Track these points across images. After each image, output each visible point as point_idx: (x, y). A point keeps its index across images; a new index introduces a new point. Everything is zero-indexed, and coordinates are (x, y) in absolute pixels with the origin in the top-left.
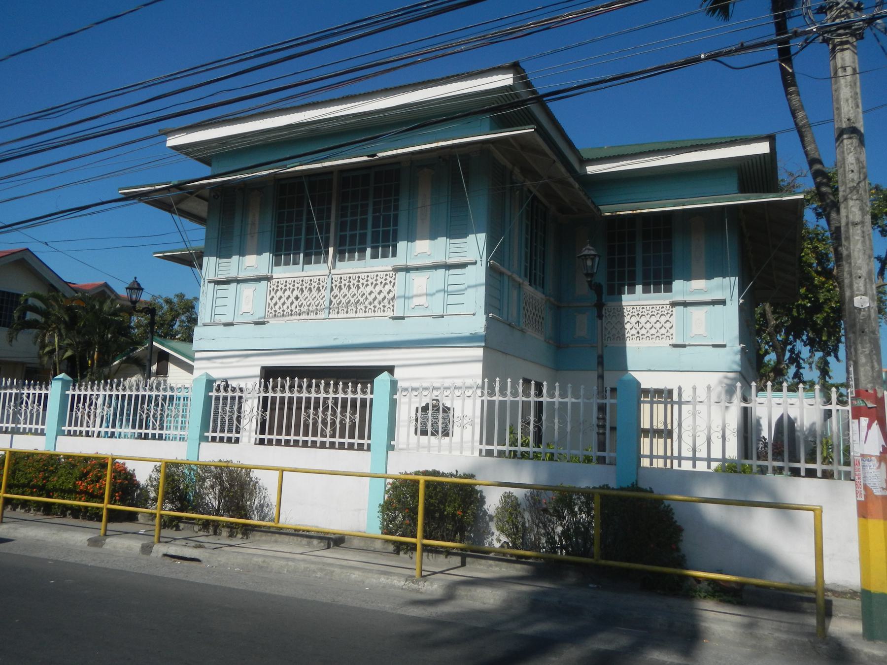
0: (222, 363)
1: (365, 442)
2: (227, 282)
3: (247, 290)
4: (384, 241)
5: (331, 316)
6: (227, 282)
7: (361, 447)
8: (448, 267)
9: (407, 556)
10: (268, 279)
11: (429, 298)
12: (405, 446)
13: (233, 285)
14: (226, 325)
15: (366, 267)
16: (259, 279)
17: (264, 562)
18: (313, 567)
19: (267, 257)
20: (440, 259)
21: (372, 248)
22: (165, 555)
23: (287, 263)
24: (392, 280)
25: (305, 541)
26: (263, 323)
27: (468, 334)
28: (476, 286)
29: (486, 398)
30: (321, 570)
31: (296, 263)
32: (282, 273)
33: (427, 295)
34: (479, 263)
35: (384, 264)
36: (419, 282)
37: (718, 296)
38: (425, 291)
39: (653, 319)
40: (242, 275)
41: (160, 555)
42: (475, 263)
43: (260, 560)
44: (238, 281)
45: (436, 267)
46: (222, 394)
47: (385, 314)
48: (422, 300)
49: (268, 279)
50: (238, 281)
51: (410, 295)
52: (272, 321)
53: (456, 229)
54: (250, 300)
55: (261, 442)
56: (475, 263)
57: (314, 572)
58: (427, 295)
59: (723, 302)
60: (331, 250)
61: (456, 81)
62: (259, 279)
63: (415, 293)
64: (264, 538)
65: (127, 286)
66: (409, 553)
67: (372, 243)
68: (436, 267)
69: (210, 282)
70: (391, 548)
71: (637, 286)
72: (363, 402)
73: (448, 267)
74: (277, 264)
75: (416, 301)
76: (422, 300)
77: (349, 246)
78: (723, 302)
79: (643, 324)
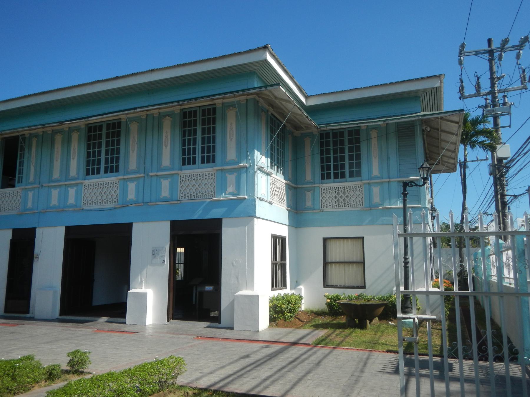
16: (268, 174)
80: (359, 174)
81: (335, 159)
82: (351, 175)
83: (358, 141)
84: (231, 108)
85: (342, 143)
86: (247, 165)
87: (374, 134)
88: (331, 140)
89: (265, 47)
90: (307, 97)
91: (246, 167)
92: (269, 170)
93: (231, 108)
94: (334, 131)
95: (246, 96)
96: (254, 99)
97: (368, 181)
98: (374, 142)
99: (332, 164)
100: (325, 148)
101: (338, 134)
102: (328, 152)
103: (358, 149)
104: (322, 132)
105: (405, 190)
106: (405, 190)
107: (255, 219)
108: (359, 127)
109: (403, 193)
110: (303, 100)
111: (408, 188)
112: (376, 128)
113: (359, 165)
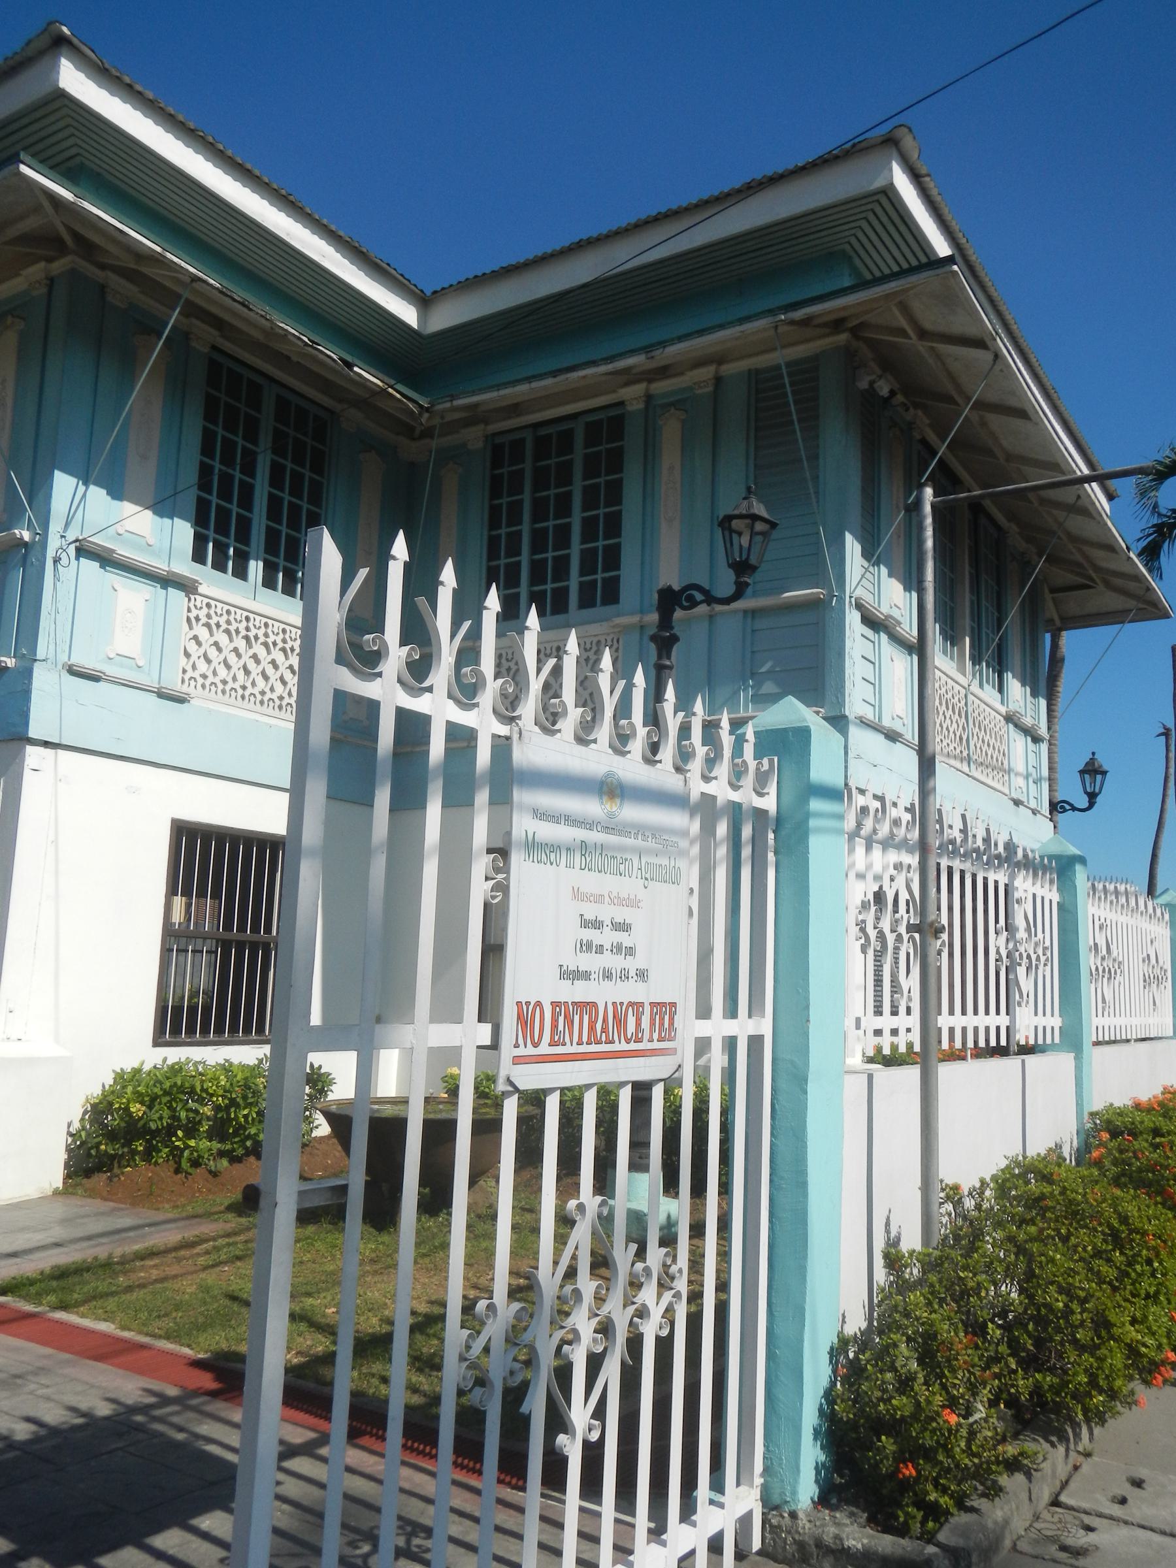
3: (134, 597)
10: (188, 587)
16: (167, 581)
19: (183, 532)
26: (180, 700)
80: (611, 595)
81: (539, 543)
82: (587, 601)
83: (616, 462)
84: (9, 320)
85: (565, 474)
86: (26, 535)
87: (671, 431)
88: (528, 466)
89: (59, 43)
90: (424, 301)
91: (26, 544)
92: (184, 567)
93: (9, 320)
94: (543, 432)
95: (42, 264)
96: (73, 272)
97: (635, 619)
98: (670, 458)
99: (525, 559)
100: (504, 501)
101: (552, 440)
102: (515, 517)
103: (615, 493)
104: (498, 440)
105: (665, 621)
106: (665, 621)
107: (30, 749)
108: (621, 404)
109: (653, 638)
110: (407, 313)
111: (679, 614)
112: (681, 403)
113: (613, 558)
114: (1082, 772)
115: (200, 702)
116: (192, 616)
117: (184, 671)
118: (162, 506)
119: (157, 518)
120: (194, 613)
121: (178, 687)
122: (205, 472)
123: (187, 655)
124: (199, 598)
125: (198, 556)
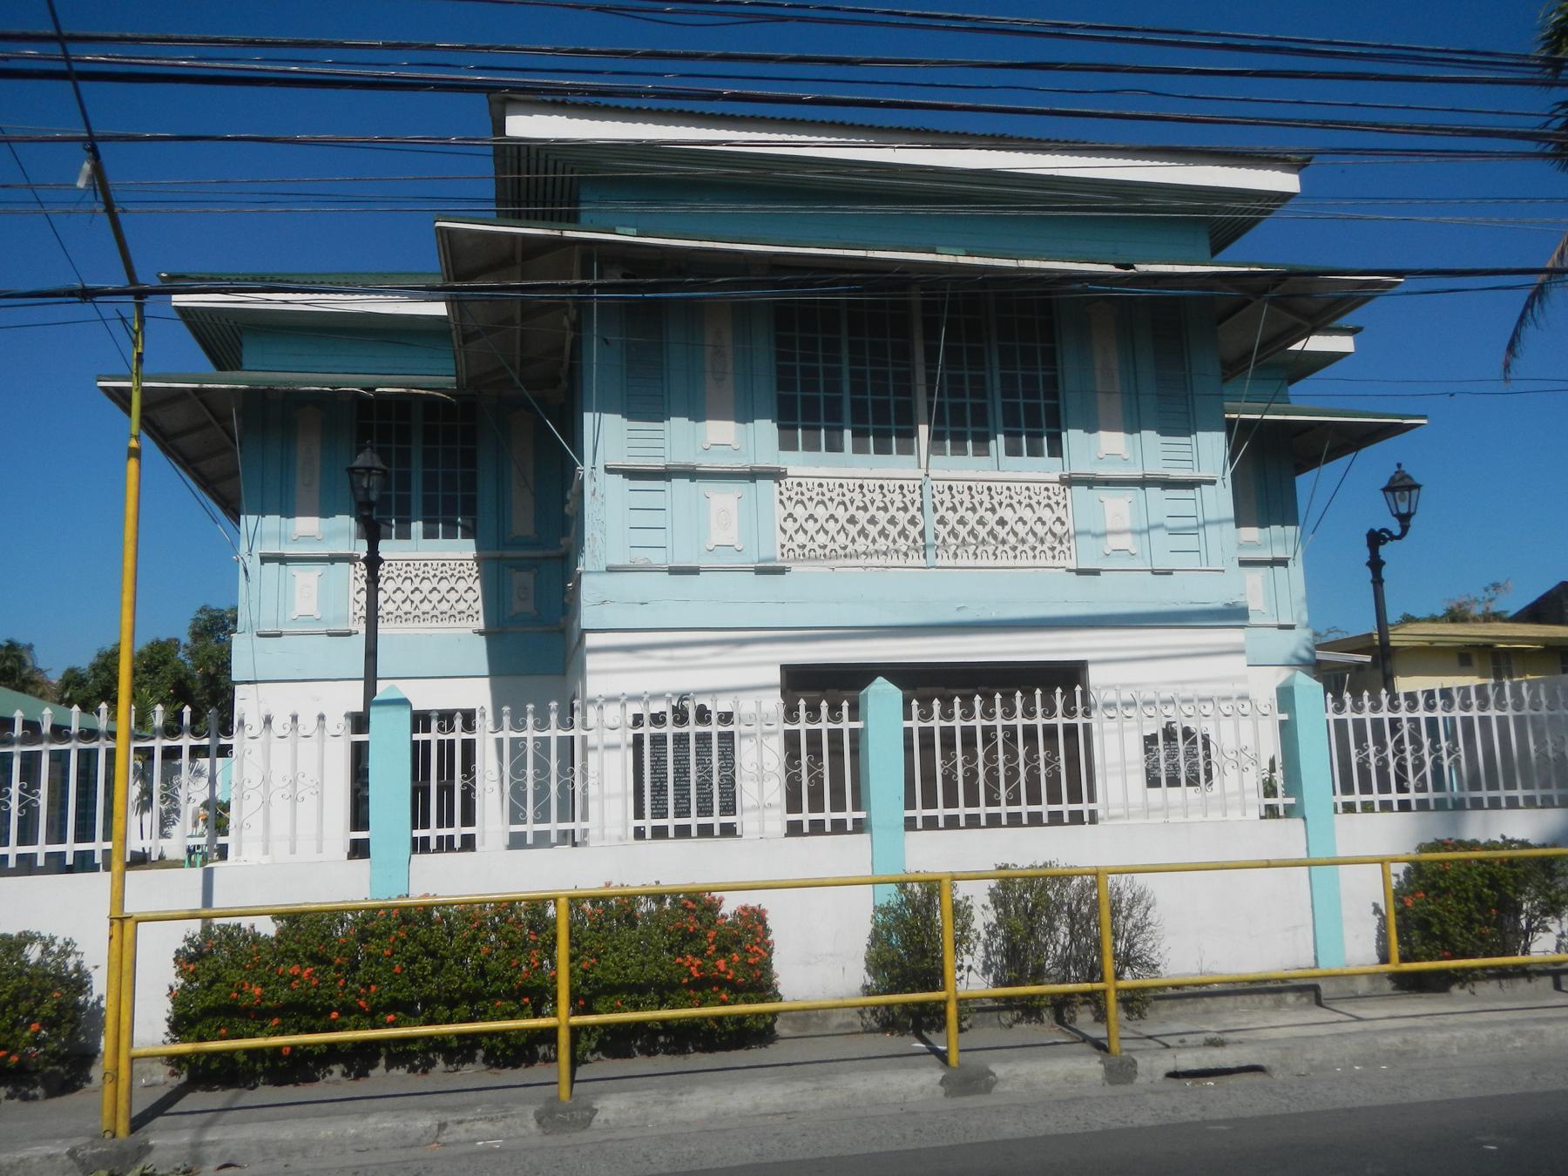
0: (671, 658)
1: (1085, 807)
2: (666, 474)
3: (723, 497)
4: (1038, 425)
5: (939, 562)
6: (666, 474)
7: (1076, 818)
8: (1167, 484)
9: (1465, 992)
10: (777, 475)
11: (1137, 537)
12: (1120, 811)
13: (677, 483)
14: (674, 571)
15: (1000, 472)
16: (753, 475)
17: (1405, 1041)
18: (1503, 1031)
19: (766, 429)
20: (1156, 469)
21: (1007, 434)
22: (1174, 1075)
23: (812, 446)
24: (1060, 499)
25: (1268, 1000)
26: (781, 571)
27: (1219, 605)
28: (1219, 522)
29: (1332, 716)
30: (1521, 1034)
31: (835, 446)
32: (803, 465)
33: (1133, 532)
34: (1220, 483)
35: (1045, 468)
36: (1118, 507)
37: (1279, 553)
38: (1127, 525)
39: (444, 586)
40: (705, 462)
41: (1160, 1076)
42: (1213, 482)
43: (1394, 1040)
44: (692, 474)
45: (1144, 483)
46: (693, 728)
47: (1056, 563)
48: (1126, 541)
49: (777, 475)
50: (692, 474)
51: (1098, 530)
52: (797, 568)
53: (1178, 419)
54: (723, 519)
55: (794, 829)
56: (1213, 482)
57: (1509, 1039)
58: (1133, 532)
59: (1283, 562)
60: (923, 430)
61: (1026, 150)
62: (753, 475)
63: (1109, 527)
64: (1179, 1009)
65: (1384, 483)
66: (1469, 986)
67: (1006, 424)
68: (1144, 483)
69: (609, 470)
70: (1387, 986)
71: (414, 525)
72: (1071, 731)
73: (1167, 484)
74: (787, 444)
75: (1114, 542)
76: (1126, 541)
77: (963, 427)
78: (1283, 562)
79: (444, 592)
114: (1385, 490)
115: (797, 568)
116: (784, 498)
117: (783, 546)
118: (744, 415)
119: (741, 426)
120: (787, 494)
121: (777, 557)
122: (781, 371)
123: (784, 531)
124: (789, 481)
125: (787, 444)
